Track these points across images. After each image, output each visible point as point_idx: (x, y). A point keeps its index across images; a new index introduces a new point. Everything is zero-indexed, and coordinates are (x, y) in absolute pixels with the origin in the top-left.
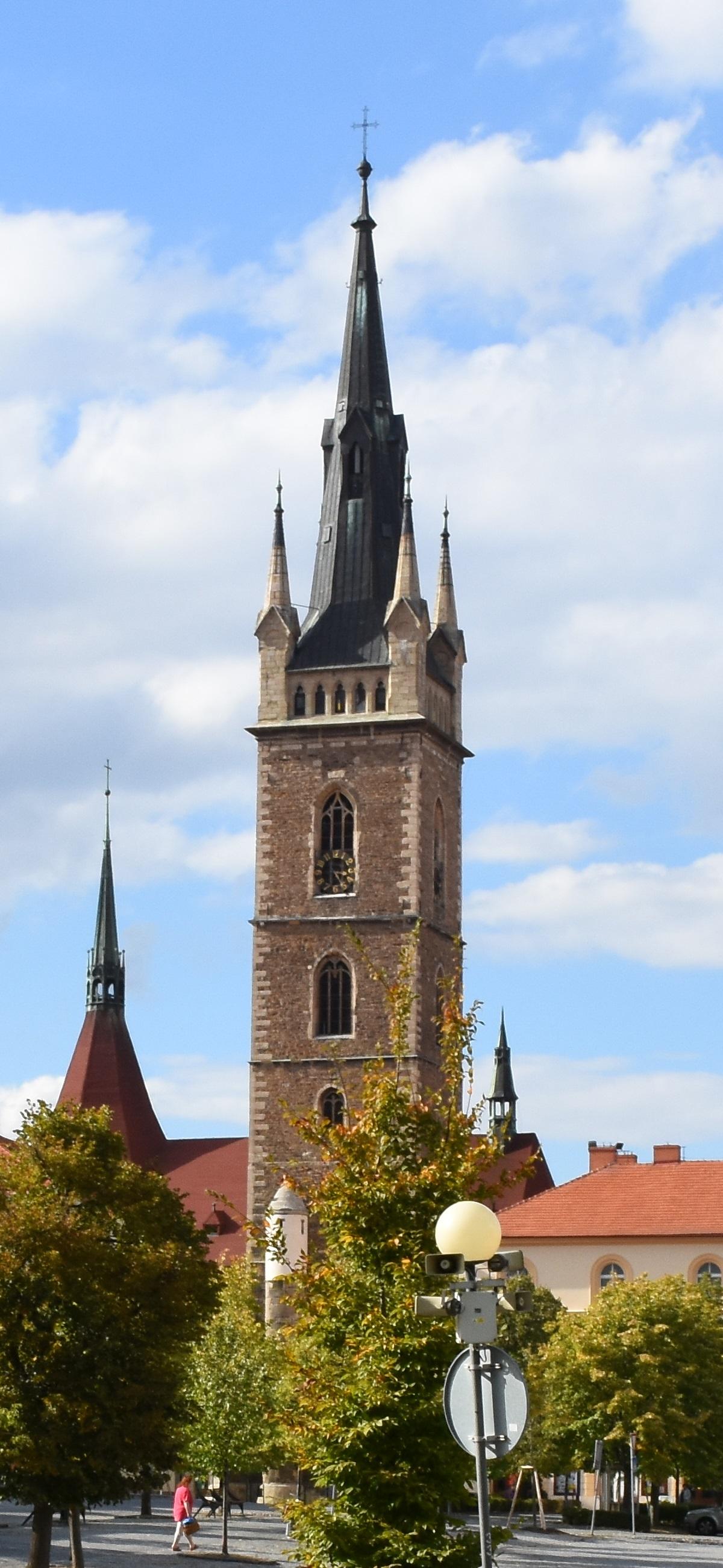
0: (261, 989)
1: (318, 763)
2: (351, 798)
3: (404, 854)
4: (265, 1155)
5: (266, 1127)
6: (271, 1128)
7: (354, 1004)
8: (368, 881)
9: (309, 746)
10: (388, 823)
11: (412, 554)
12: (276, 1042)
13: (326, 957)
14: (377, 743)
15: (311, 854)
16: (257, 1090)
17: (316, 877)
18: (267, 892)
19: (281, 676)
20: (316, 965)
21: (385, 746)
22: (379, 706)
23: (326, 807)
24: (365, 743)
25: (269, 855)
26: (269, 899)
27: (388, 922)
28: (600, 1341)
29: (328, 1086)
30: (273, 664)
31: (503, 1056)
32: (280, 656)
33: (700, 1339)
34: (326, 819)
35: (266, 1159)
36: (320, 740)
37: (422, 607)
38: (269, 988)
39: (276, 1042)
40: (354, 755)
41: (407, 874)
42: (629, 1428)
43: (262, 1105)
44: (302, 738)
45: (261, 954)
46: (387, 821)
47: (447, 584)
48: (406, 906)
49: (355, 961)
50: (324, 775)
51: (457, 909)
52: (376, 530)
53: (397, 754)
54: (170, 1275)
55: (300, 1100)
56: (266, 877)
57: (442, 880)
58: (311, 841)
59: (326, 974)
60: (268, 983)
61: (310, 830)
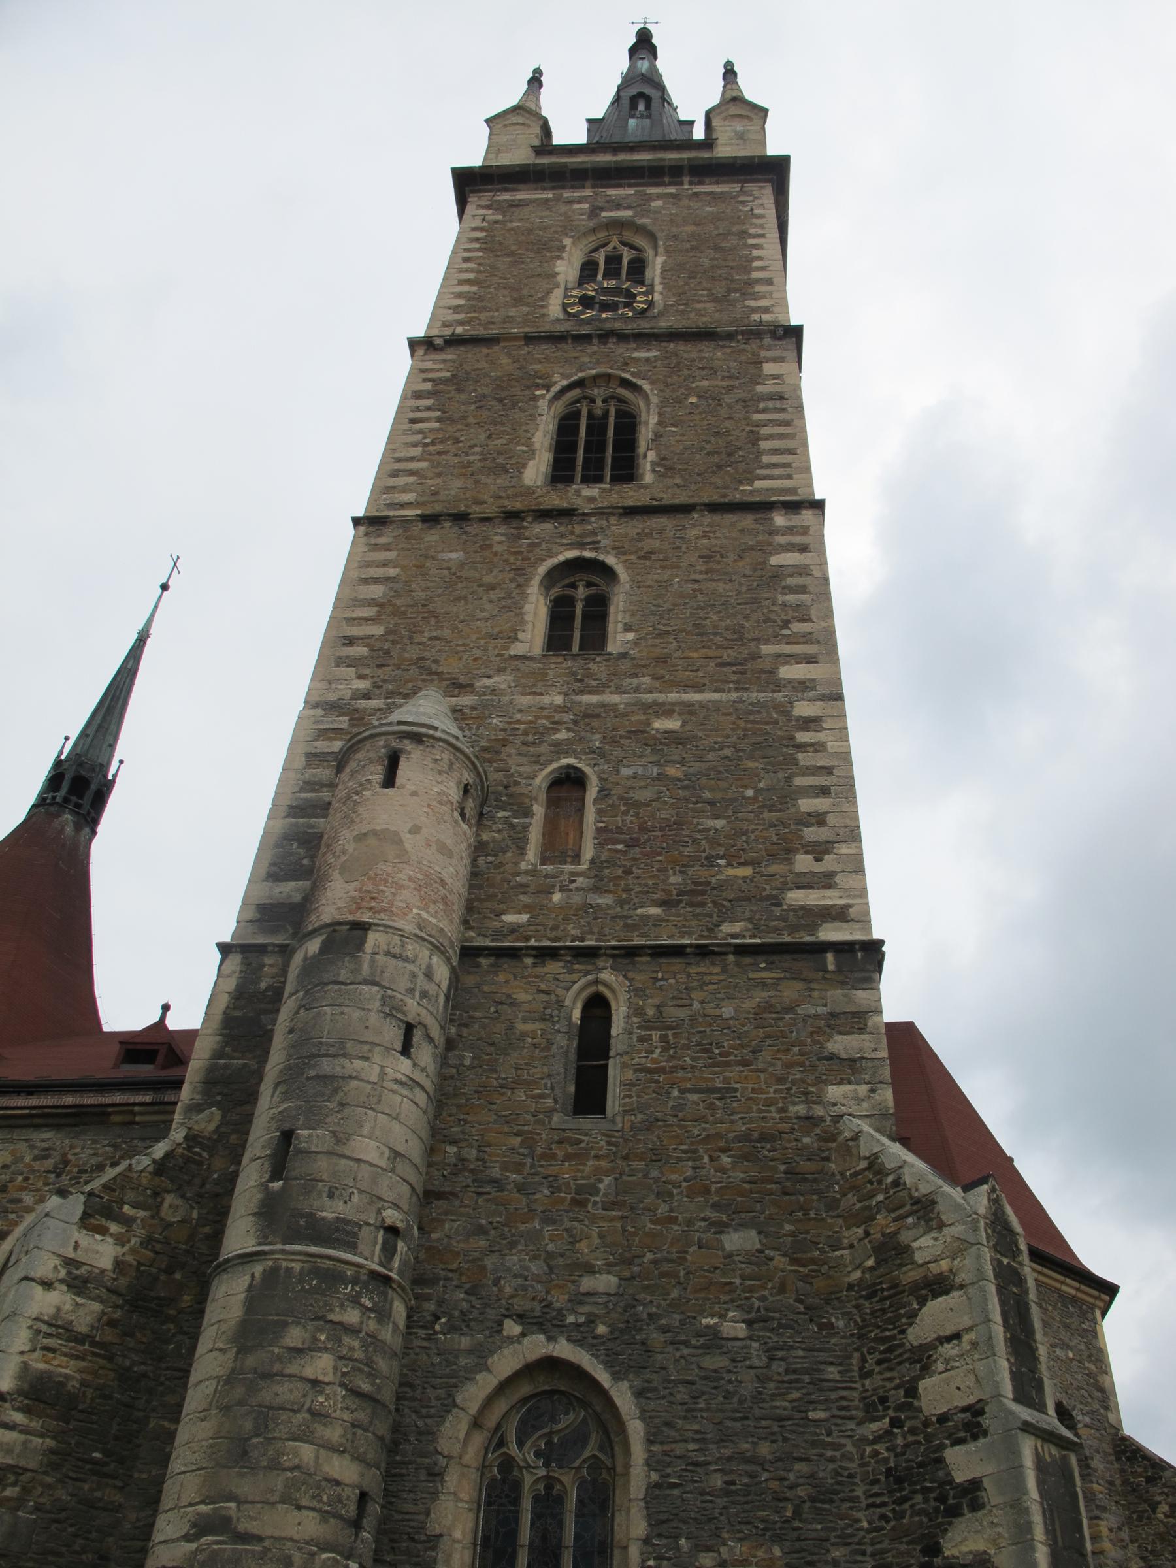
2: (640, 241)
4: (362, 685)
9: (565, 195)
13: (580, 383)
16: (368, 564)
17: (564, 307)
20: (556, 389)
35: (367, 696)
38: (439, 420)
39: (435, 493)
45: (425, 380)
49: (652, 383)
55: (488, 579)
59: (576, 415)
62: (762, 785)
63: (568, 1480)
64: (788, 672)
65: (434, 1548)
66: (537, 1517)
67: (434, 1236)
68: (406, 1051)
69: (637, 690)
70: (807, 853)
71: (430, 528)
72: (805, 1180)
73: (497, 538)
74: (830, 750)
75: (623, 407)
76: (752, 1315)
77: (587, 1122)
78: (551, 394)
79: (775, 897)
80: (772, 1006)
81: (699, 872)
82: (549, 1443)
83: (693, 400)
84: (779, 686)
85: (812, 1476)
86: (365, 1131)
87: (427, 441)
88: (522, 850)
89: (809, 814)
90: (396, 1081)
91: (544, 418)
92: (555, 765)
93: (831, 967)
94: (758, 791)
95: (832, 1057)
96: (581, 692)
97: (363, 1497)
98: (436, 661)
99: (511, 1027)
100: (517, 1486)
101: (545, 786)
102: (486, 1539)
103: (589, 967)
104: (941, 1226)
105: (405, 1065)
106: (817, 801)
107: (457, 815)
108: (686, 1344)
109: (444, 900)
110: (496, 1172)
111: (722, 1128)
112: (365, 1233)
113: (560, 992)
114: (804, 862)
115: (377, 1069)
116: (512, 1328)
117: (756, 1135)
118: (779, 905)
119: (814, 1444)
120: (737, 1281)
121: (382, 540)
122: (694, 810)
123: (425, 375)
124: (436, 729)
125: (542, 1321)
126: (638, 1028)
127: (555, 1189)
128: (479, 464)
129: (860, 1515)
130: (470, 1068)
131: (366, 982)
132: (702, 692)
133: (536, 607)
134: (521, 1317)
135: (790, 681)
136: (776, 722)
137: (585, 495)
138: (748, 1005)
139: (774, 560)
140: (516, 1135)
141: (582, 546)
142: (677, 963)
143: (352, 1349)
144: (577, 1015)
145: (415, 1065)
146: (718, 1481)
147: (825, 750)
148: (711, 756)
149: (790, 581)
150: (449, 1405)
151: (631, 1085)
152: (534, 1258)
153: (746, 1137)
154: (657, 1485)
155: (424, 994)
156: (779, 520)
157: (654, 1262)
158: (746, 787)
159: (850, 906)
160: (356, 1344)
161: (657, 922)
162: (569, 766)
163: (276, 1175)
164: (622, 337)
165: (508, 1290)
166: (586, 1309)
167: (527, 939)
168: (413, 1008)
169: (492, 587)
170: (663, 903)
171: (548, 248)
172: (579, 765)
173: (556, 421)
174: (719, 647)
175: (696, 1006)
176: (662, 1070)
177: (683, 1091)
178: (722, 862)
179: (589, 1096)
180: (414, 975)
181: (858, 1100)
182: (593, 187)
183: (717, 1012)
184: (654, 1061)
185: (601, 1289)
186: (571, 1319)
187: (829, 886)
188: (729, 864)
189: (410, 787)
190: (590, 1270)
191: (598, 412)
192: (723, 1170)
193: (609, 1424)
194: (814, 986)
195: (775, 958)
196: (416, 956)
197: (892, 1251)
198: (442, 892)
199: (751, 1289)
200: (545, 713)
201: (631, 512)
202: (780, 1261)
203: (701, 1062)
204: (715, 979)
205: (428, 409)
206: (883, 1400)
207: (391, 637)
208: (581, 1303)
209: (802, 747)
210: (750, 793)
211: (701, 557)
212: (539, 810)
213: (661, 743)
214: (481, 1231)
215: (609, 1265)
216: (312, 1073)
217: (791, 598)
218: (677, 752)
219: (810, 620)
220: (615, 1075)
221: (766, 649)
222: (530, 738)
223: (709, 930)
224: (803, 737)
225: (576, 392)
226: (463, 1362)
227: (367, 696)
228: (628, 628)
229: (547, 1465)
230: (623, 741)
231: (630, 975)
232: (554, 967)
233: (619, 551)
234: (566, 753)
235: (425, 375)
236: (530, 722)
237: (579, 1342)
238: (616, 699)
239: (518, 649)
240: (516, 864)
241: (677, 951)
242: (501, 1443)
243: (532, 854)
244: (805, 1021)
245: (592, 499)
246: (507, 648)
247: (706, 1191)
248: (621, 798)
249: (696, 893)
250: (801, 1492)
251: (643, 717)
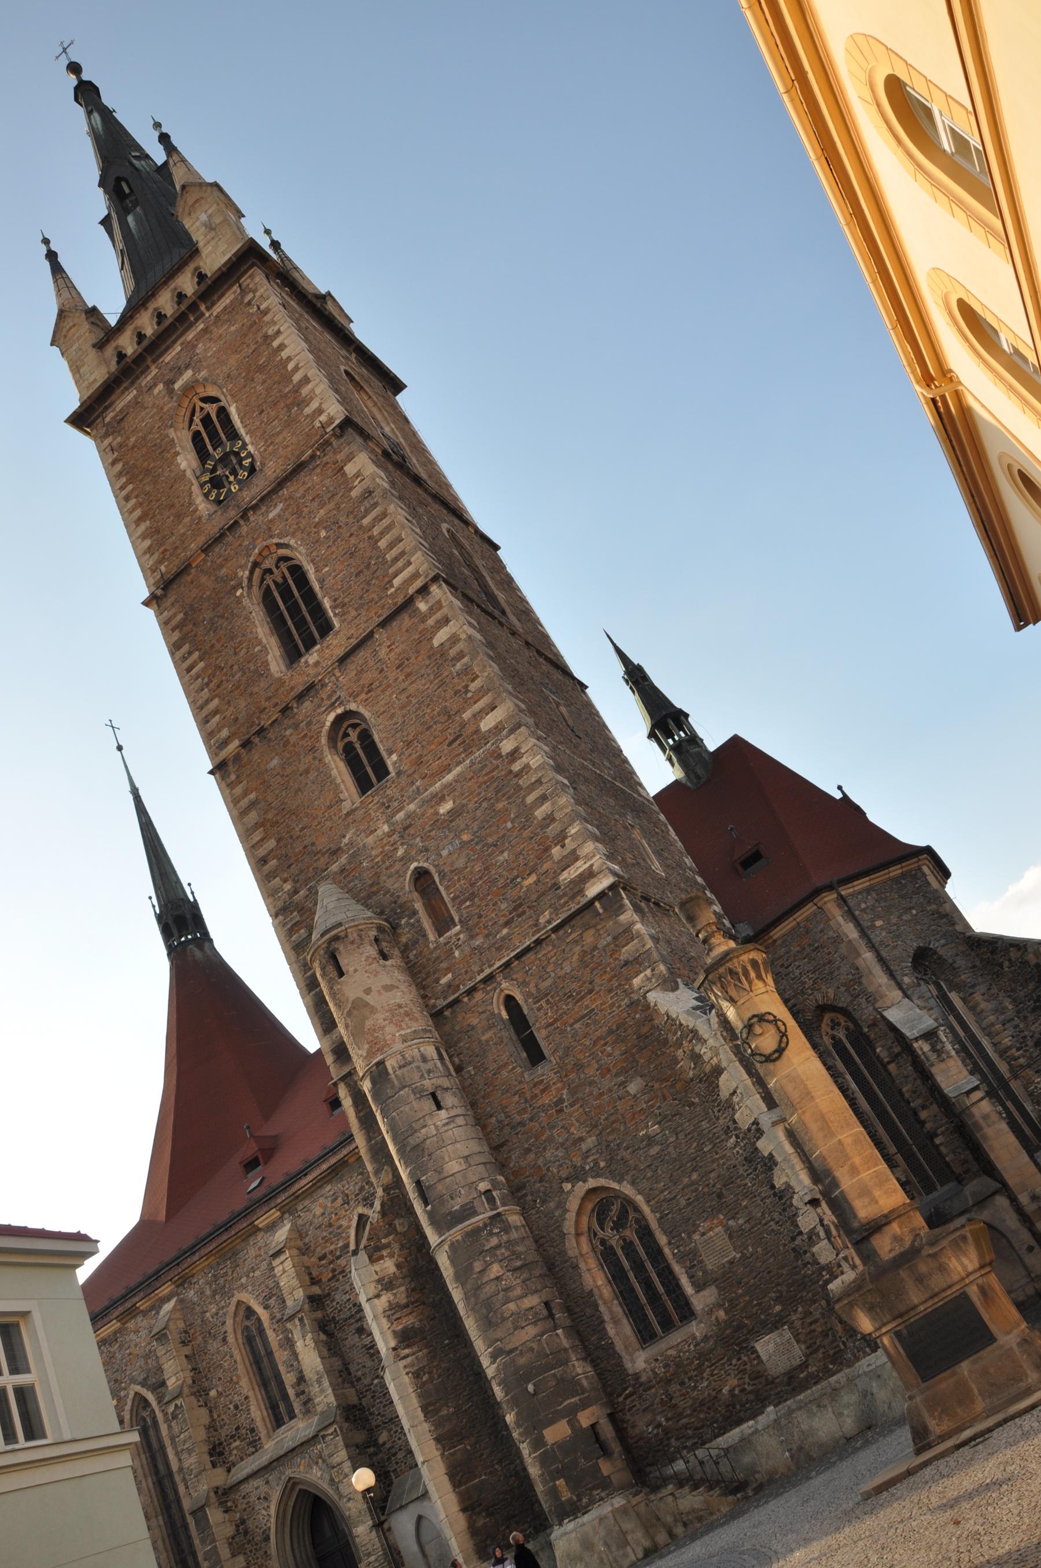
0: (189, 670)
1: (161, 386)
2: (212, 391)
3: (297, 378)
4: (288, 887)
5: (272, 843)
6: (279, 840)
7: (316, 587)
9: (143, 384)
10: (261, 369)
12: (236, 720)
13: (256, 565)
14: (215, 314)
15: (189, 474)
17: (206, 496)
18: (156, 556)
19: (92, 354)
21: (225, 308)
23: (191, 421)
24: (202, 326)
25: (139, 521)
26: (160, 562)
27: (313, 457)
29: (331, 717)
30: (80, 353)
31: (636, 677)
34: (197, 435)
36: (153, 367)
39: (236, 720)
40: (195, 346)
41: (313, 390)
43: (253, 816)
44: (132, 383)
45: (173, 630)
49: (293, 535)
50: (171, 392)
53: (241, 303)
55: (302, 768)
56: (147, 543)
58: (187, 461)
60: (197, 654)
61: (177, 454)
62: (512, 816)
63: (631, 1234)
64: (487, 723)
65: (593, 1296)
66: (627, 1256)
67: (511, 1165)
68: (439, 1107)
69: (418, 792)
70: (556, 845)
71: (250, 750)
72: (647, 1037)
73: (288, 732)
74: (534, 767)
75: (290, 563)
76: (659, 1119)
77: (540, 1069)
78: (246, 589)
79: (555, 884)
80: (585, 952)
81: (512, 894)
82: (613, 1222)
83: (323, 534)
84: (485, 738)
85: (719, 1176)
86: (447, 1159)
87: (206, 680)
88: (425, 936)
89: (544, 819)
90: (444, 1125)
91: (254, 614)
92: (409, 873)
93: (601, 911)
94: (512, 822)
95: (627, 963)
96: (394, 815)
97: (547, 1304)
98: (313, 844)
99: (480, 1041)
100: (611, 1247)
101: (413, 888)
102: (613, 1276)
103: (495, 985)
104: (705, 1041)
105: (443, 1114)
106: (544, 807)
107: (382, 962)
108: (639, 1148)
109: (407, 1014)
110: (518, 1118)
111: (598, 1034)
112: (476, 1203)
113: (489, 1008)
114: (556, 851)
115: (432, 1127)
116: (567, 1186)
117: (614, 1027)
118: (559, 888)
119: (713, 1162)
120: (644, 1106)
121: (233, 777)
122: (490, 855)
123: (170, 626)
124: (340, 924)
125: (577, 1176)
126: (535, 1003)
127: (546, 1111)
128: (245, 678)
129: (747, 1181)
130: (476, 1074)
131: (401, 1089)
132: (450, 771)
133: (337, 767)
134: (567, 1179)
135: (489, 731)
136: (498, 767)
137: (312, 657)
138: (576, 957)
139: (436, 643)
140: (515, 1095)
141: (332, 707)
142: (531, 956)
143: (503, 1254)
144: (505, 1015)
145: (447, 1109)
146: (683, 1202)
147: (531, 768)
148: (479, 813)
149: (453, 652)
150: (563, 1235)
151: (548, 1037)
152: (557, 1149)
153: (611, 1032)
154: (661, 1218)
155: (429, 1072)
156: (422, 606)
157: (606, 1119)
158: (506, 822)
159: (592, 865)
160: (503, 1250)
161: (507, 938)
162: (416, 868)
163: (426, 1203)
164: (255, 508)
165: (555, 1171)
166: (591, 1158)
167: (458, 986)
168: (428, 1084)
169: (307, 771)
170: (507, 924)
171: (165, 450)
172: (421, 865)
173: (261, 605)
174: (442, 731)
175: (553, 974)
176: (556, 1020)
177: (571, 1026)
178: (519, 880)
179: (535, 1055)
180: (418, 1068)
181: (649, 979)
182: (154, 362)
183: (563, 972)
184: (551, 1018)
185: (592, 1146)
186: (587, 1167)
187: (577, 859)
188: (523, 879)
189: (351, 969)
190: (581, 1139)
191: (280, 580)
192: (610, 1055)
193: (628, 1204)
194: (599, 927)
195: (572, 923)
196: (413, 1057)
197: (696, 1058)
198: (402, 1011)
199: (652, 1106)
200: (385, 841)
201: (342, 660)
202: (657, 1086)
203: (570, 1006)
204: (552, 953)
205: (190, 653)
206: (728, 1127)
207: (282, 844)
208: (587, 1157)
209: (518, 775)
210: (509, 825)
211: (397, 668)
212: (418, 906)
213: (451, 821)
214: (528, 1151)
215: (588, 1132)
216: (409, 1148)
217: (458, 666)
218: (460, 822)
219: (477, 676)
220: (540, 1036)
221: (467, 715)
222: (388, 864)
223: (536, 925)
224: (516, 767)
225: (258, 572)
226: (557, 1214)
227: (296, 892)
228: (390, 753)
229: (618, 1231)
230: (433, 833)
231: (514, 977)
232: (479, 996)
233: (354, 695)
234: (411, 860)
235: (170, 626)
236: (382, 853)
237: (597, 1176)
238: (412, 807)
239: (347, 806)
240: (428, 946)
241: (528, 950)
242: (595, 1234)
243: (432, 936)
244: (605, 950)
245: (317, 664)
246: (340, 810)
247: (609, 1070)
248: (452, 871)
249: (518, 907)
250: (718, 1186)
251: (432, 811)
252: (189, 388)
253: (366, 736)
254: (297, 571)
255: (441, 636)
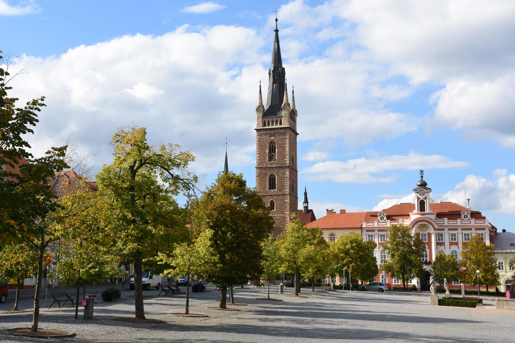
8: (279, 159)
10: (283, 147)
11: (287, 94)
19: (261, 119)
22: (281, 124)
28: (341, 247)
31: (306, 194)
32: (261, 115)
33: (362, 247)
37: (289, 104)
42: (349, 267)
46: (283, 147)
47: (294, 101)
48: (287, 164)
51: (296, 165)
52: (280, 90)
54: (261, 219)
57: (293, 159)
58: (267, 151)
252: (272, 140)
253: (274, 204)
254: (275, 178)
255: (286, 200)
